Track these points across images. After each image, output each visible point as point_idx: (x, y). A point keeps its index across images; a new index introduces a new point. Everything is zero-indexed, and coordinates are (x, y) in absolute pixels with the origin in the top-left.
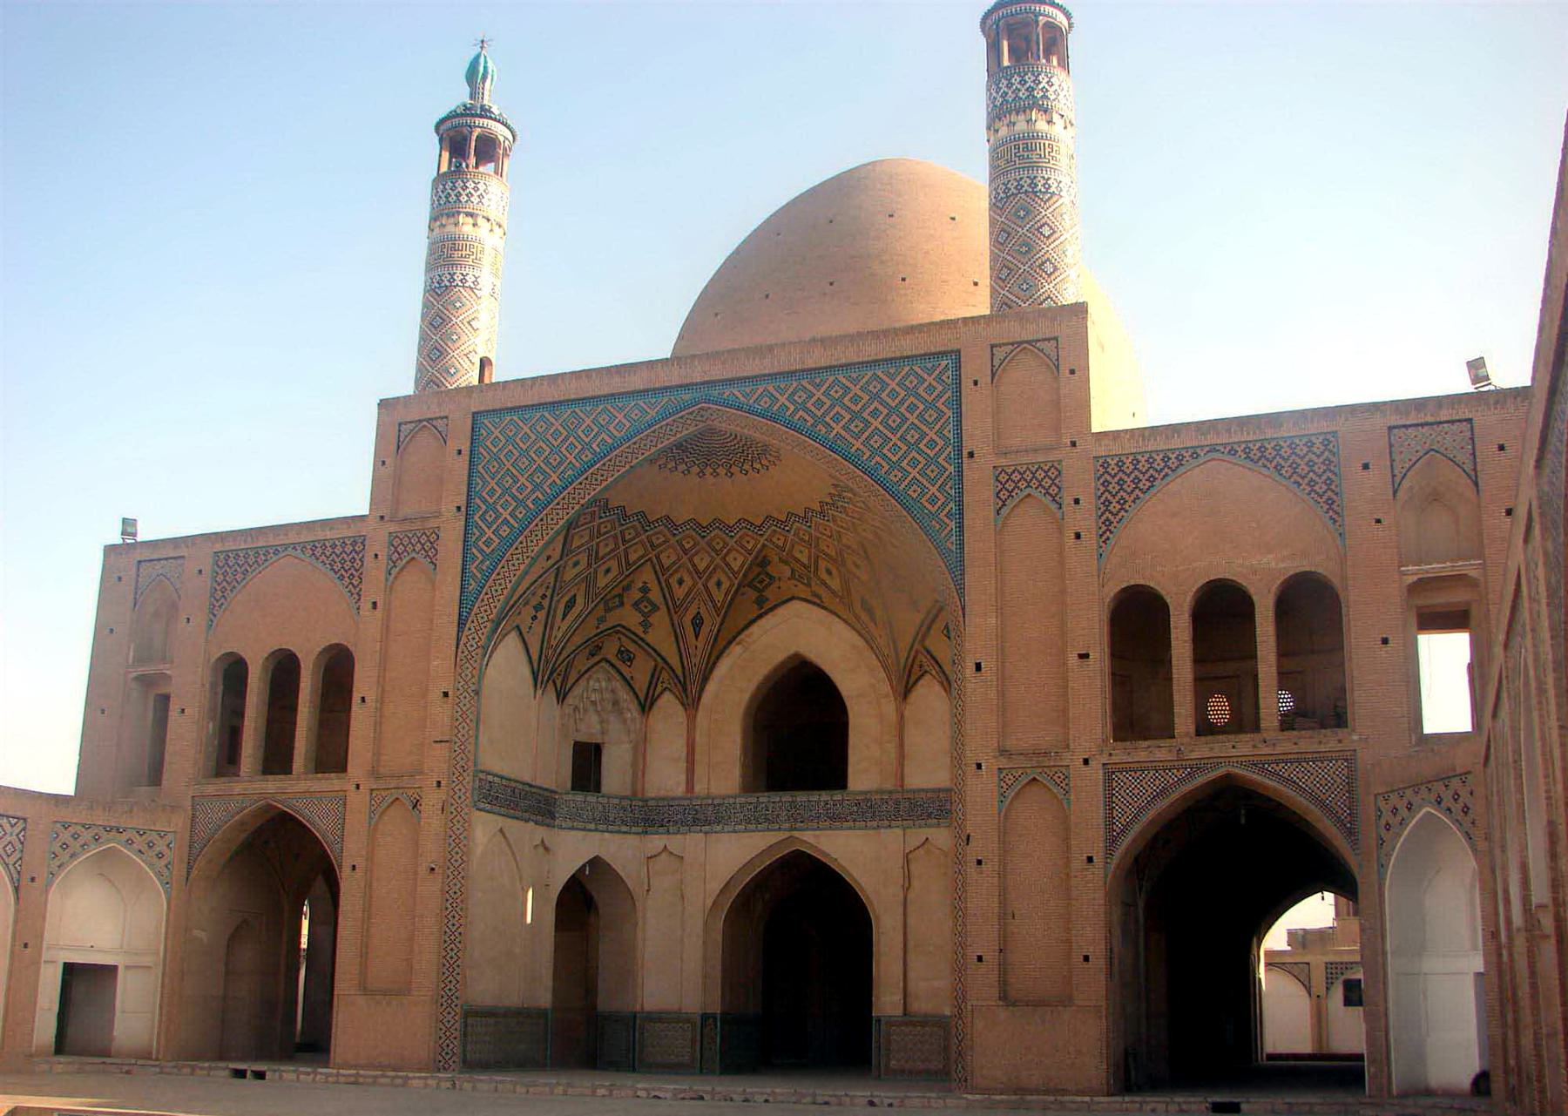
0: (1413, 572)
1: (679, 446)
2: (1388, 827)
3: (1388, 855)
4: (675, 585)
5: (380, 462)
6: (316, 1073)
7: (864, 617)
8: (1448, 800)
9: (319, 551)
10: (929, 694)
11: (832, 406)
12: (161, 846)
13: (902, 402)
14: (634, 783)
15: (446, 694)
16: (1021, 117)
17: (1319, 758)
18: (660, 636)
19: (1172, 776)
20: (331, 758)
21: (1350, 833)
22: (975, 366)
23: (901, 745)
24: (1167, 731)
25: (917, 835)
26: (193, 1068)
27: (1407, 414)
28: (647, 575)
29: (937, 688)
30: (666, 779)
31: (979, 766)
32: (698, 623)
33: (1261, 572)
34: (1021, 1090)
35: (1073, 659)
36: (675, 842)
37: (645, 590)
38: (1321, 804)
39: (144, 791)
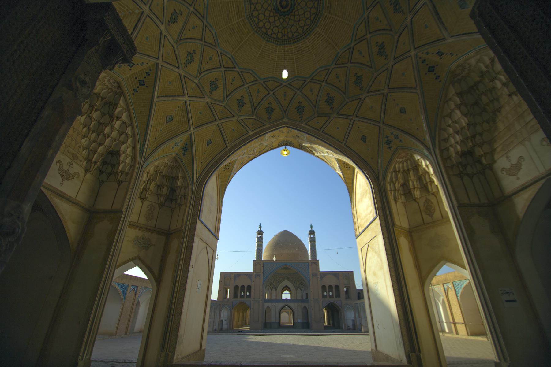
5: (254, 267)
10: (299, 290)
20: (249, 297)
22: (310, 264)
30: (274, 298)
36: (275, 304)
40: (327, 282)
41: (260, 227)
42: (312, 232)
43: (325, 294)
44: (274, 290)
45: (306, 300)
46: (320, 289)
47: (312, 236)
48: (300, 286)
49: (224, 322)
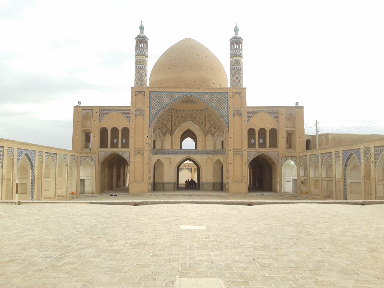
0: (287, 129)
1: (183, 100)
2: (283, 161)
3: (283, 164)
4: (174, 118)
5: (132, 98)
6: (127, 195)
7: (201, 124)
8: (293, 159)
9: (121, 111)
10: (209, 136)
11: (209, 98)
12: (94, 159)
13: (220, 99)
14: (162, 147)
15: (147, 136)
16: (237, 57)
17: (274, 152)
18: (169, 126)
19: (255, 153)
20: (126, 145)
21: (278, 161)
22: (230, 95)
23: (205, 143)
24: (255, 147)
25: (208, 156)
26: (102, 195)
27: (287, 108)
28: (170, 117)
29: (211, 135)
30: (167, 147)
31: (230, 151)
32: (175, 123)
33: (268, 127)
34: (237, 193)
35: (243, 137)
36: (170, 156)
37: (169, 119)
38: (274, 157)
39: (86, 150)
40: (257, 124)
41: (142, 28)
42: (236, 42)
43: (253, 141)
44: (168, 136)
45: (222, 151)
46: (246, 134)
47: (236, 46)
48: (212, 129)
49: (87, 183)
